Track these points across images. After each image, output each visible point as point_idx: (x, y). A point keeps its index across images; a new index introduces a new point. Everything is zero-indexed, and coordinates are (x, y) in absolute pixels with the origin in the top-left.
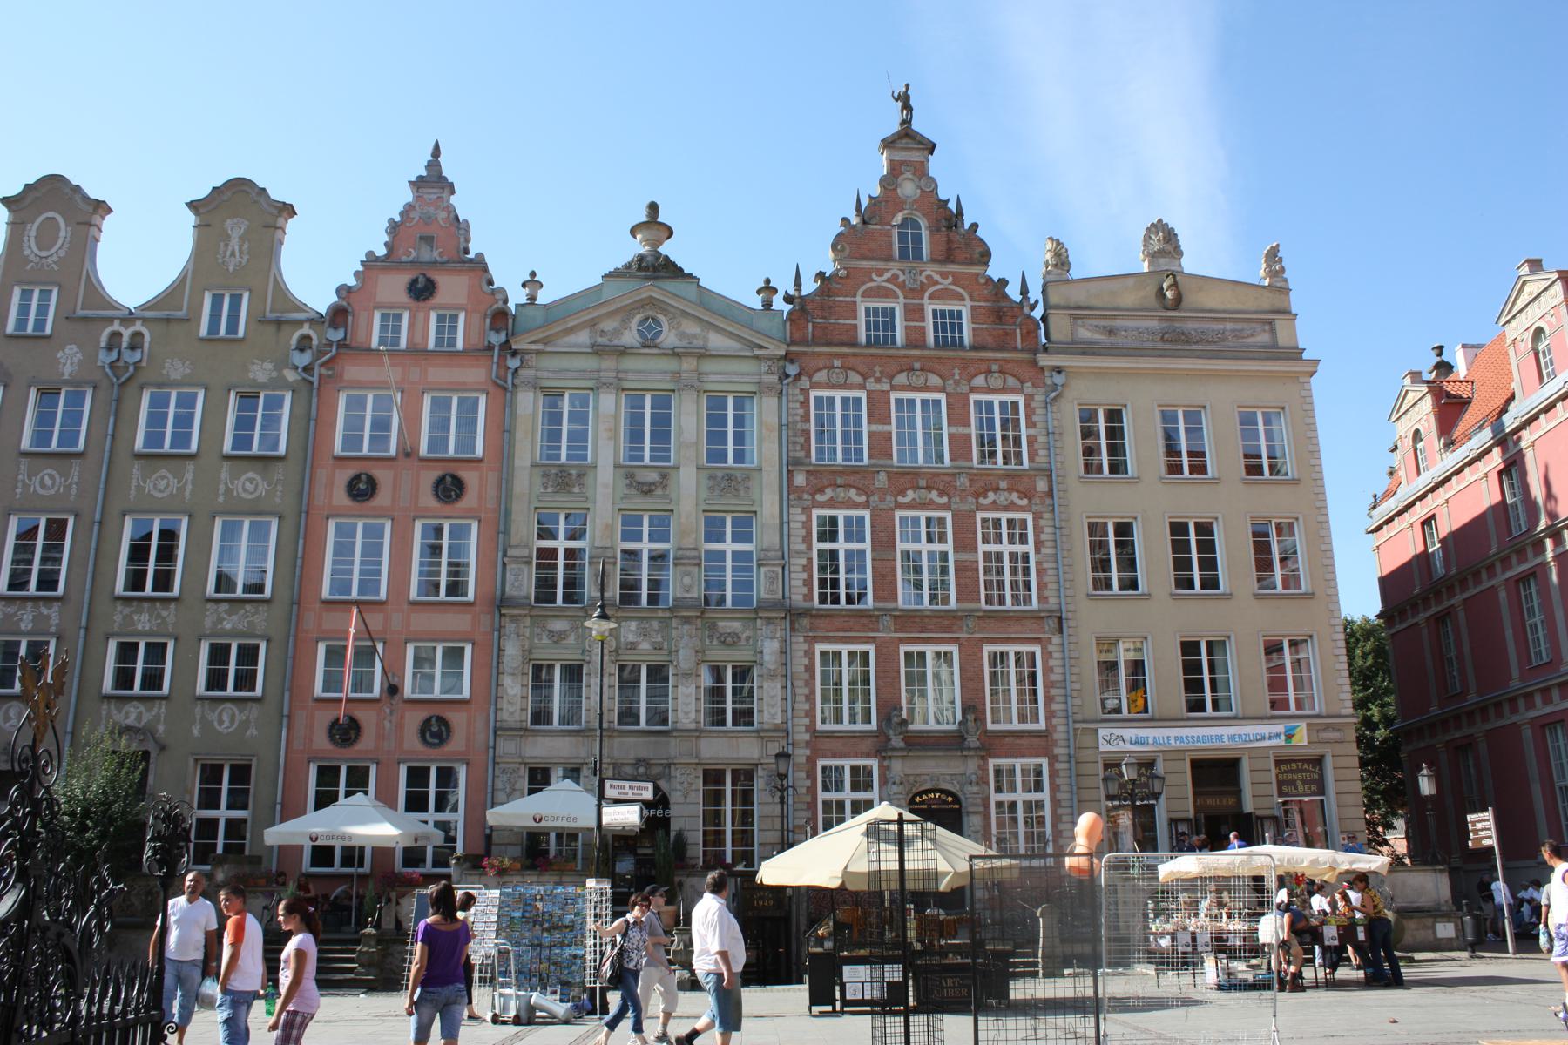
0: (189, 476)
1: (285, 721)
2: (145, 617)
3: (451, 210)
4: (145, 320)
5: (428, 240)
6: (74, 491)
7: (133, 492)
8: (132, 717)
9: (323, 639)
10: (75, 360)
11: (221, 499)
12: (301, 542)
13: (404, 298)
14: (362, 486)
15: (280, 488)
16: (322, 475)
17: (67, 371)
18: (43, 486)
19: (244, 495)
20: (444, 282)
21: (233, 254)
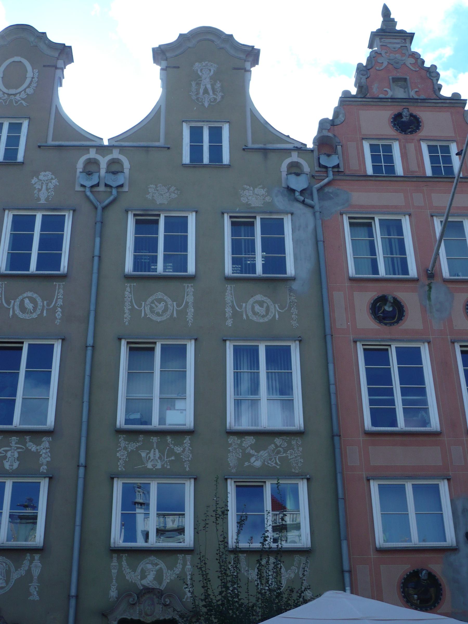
0: (190, 299)
1: (347, 575)
2: (155, 454)
3: (416, 56)
4: (122, 149)
5: (400, 81)
6: (59, 314)
7: (127, 315)
8: (151, 577)
9: (375, 478)
10: (51, 186)
11: (229, 323)
12: (331, 366)
13: (390, 131)
14: (388, 308)
15: (294, 310)
16: (339, 298)
17: (43, 197)
18: (23, 309)
19: (255, 319)
20: (426, 116)
21: (206, 91)
